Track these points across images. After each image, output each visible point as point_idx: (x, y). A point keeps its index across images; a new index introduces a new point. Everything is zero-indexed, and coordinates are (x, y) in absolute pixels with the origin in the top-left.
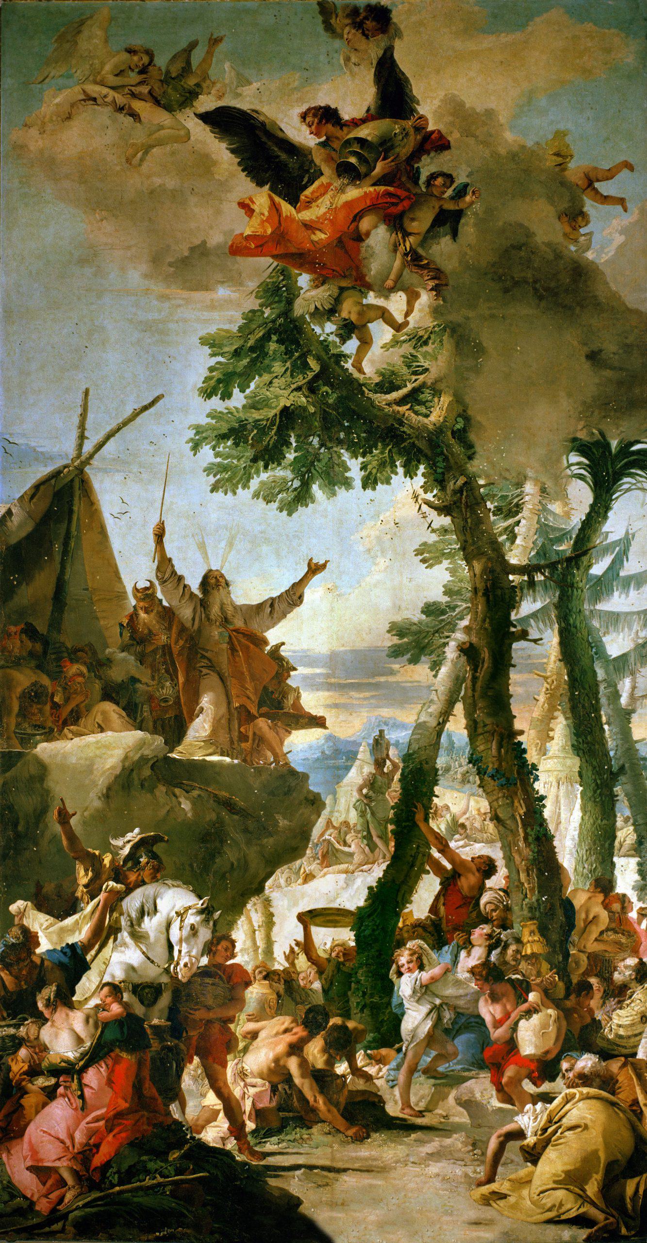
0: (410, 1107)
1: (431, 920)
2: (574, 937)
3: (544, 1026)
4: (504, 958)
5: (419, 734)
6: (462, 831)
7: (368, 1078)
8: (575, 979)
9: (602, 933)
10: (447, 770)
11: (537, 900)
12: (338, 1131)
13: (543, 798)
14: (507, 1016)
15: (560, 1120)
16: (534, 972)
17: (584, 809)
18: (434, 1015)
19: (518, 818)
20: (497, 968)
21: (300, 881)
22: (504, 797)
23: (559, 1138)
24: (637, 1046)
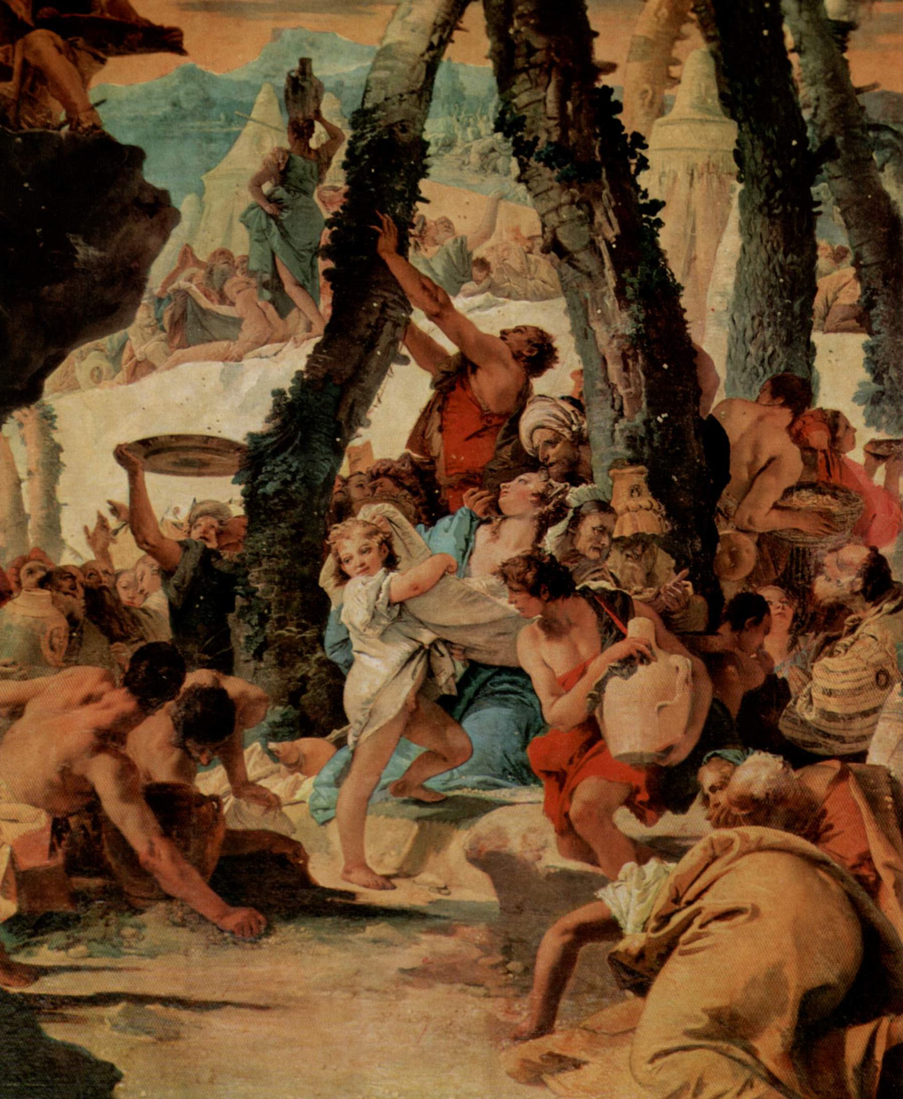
0: (364, 866)
1: (412, 463)
2: (727, 500)
3: (666, 692)
4: (572, 543)
5: (386, 68)
6: (476, 272)
7: (271, 803)
8: (730, 589)
9: (788, 492)
10: (448, 145)
11: (646, 422)
12: (203, 918)
13: (657, 205)
14: (581, 671)
15: (699, 896)
16: (640, 576)
17: (746, 229)
18: (418, 666)
19: (603, 247)
20: (558, 565)
21: (121, 376)
22: (572, 202)
23: (698, 937)
24: (864, 738)
